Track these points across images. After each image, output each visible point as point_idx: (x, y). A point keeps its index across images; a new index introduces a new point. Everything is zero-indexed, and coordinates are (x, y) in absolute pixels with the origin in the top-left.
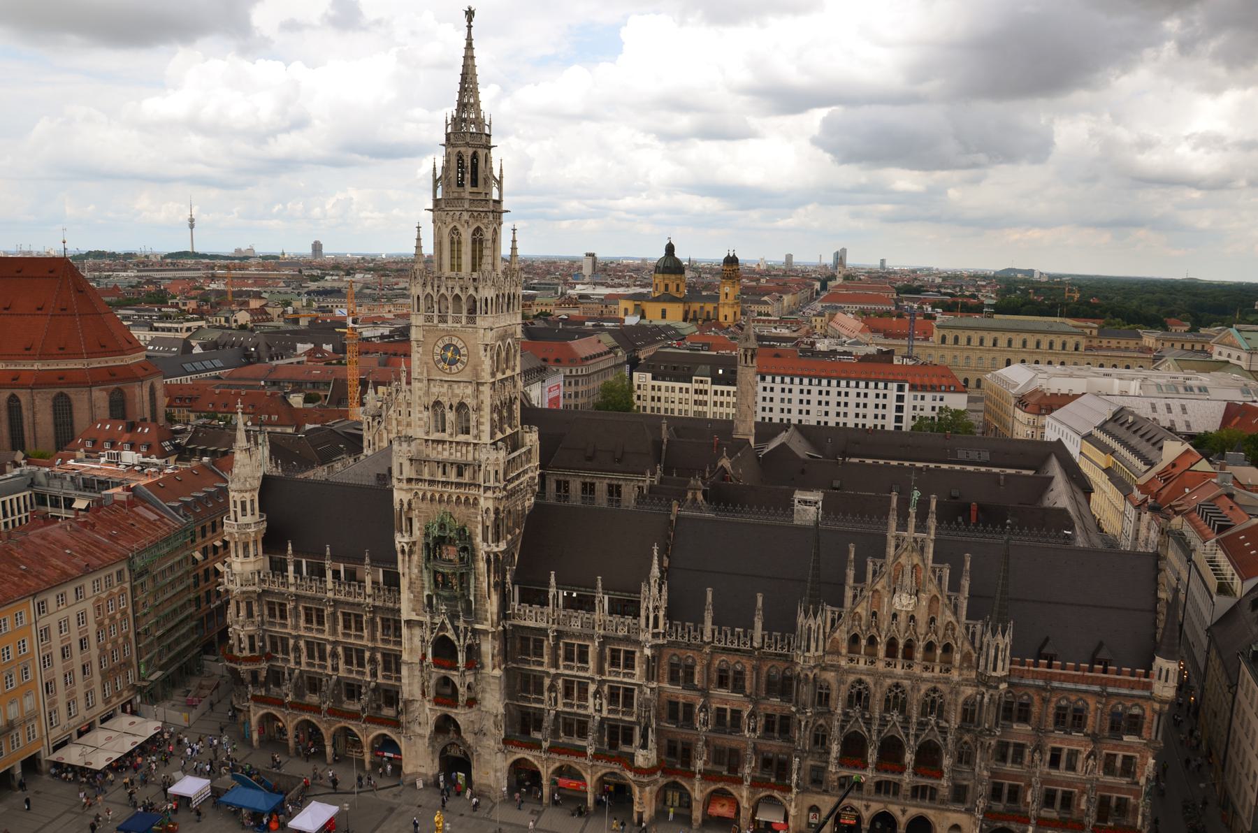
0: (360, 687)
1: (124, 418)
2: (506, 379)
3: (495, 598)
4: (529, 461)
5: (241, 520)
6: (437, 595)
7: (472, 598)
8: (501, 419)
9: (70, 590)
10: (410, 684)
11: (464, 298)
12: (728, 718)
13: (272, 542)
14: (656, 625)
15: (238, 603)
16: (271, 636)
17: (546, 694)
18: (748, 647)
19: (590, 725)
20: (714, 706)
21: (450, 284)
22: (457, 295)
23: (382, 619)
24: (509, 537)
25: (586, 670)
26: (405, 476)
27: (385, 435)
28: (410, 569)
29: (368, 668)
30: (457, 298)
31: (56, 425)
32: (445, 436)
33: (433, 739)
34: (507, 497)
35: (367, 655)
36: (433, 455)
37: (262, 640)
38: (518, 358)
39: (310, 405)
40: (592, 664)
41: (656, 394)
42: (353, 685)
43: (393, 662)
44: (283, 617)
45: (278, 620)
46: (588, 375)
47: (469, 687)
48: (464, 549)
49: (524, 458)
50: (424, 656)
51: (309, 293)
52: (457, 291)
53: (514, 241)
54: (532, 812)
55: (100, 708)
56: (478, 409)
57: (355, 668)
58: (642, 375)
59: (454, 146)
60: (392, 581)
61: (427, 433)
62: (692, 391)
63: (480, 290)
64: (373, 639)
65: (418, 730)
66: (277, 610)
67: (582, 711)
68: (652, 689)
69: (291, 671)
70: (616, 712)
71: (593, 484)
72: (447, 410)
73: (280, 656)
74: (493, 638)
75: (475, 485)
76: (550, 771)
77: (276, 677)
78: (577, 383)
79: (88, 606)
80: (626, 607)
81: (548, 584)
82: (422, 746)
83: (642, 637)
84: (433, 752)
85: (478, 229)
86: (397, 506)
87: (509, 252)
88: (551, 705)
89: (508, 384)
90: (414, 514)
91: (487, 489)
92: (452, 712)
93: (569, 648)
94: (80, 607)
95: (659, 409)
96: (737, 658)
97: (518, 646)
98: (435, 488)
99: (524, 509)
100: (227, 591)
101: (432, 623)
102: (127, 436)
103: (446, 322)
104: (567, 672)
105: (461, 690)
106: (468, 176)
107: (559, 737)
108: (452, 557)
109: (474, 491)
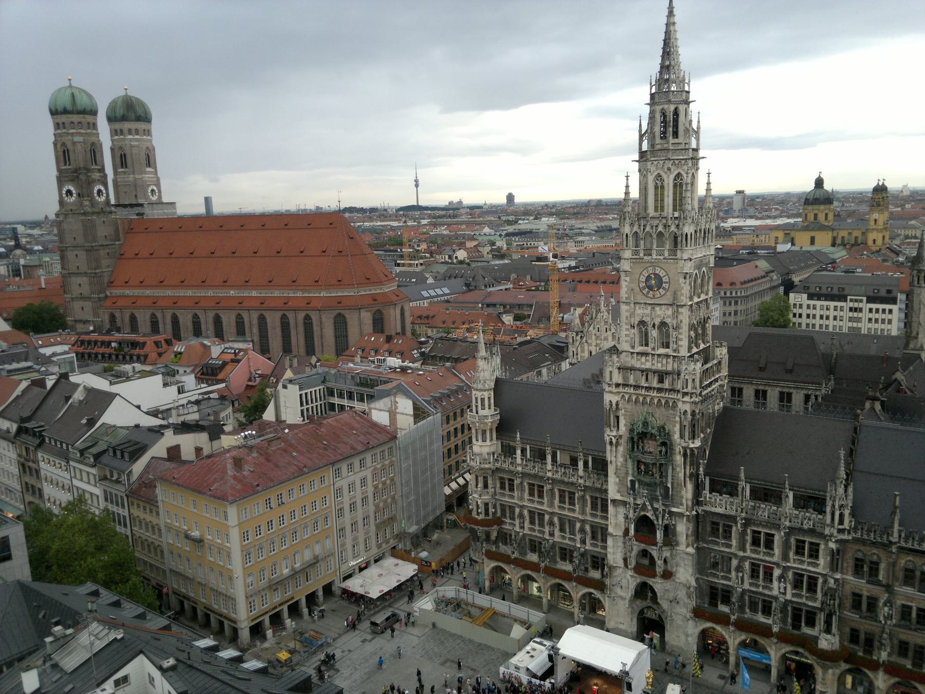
1: (383, 332)
3: (690, 486)
4: (719, 371)
6: (639, 481)
7: (669, 485)
8: (696, 336)
9: (356, 462)
10: (615, 553)
11: (667, 235)
13: (503, 429)
14: (841, 522)
16: (501, 505)
17: (733, 574)
19: (774, 604)
20: (899, 602)
21: (655, 222)
23: (591, 497)
24: (702, 435)
27: (586, 348)
28: (616, 458)
29: (578, 537)
30: (660, 235)
31: (336, 337)
33: (631, 602)
34: (702, 402)
35: (578, 525)
36: (638, 365)
37: (495, 507)
38: (711, 284)
39: (518, 323)
40: (777, 551)
41: (811, 312)
42: (565, 549)
43: (600, 533)
44: (511, 489)
45: (507, 492)
46: (747, 297)
47: (665, 561)
48: (663, 444)
50: (627, 532)
51: (508, 235)
52: (660, 228)
53: (709, 183)
55: (374, 551)
56: (677, 328)
58: (798, 295)
59: (659, 104)
60: (601, 466)
61: (633, 347)
62: (846, 309)
64: (583, 512)
65: (619, 591)
67: (767, 592)
68: (836, 580)
69: (518, 533)
70: (799, 596)
71: (765, 392)
72: (671, 330)
73: (508, 521)
74: (688, 520)
76: (737, 642)
77: (504, 537)
78: (736, 303)
79: (368, 473)
80: (812, 501)
85: (679, 175)
89: (703, 306)
90: (621, 413)
91: (685, 394)
92: (651, 581)
94: (362, 474)
95: (814, 325)
97: (709, 529)
98: (639, 392)
99: (714, 412)
101: (635, 504)
102: (386, 346)
103: (650, 255)
104: (754, 556)
105: (659, 563)
107: (744, 612)
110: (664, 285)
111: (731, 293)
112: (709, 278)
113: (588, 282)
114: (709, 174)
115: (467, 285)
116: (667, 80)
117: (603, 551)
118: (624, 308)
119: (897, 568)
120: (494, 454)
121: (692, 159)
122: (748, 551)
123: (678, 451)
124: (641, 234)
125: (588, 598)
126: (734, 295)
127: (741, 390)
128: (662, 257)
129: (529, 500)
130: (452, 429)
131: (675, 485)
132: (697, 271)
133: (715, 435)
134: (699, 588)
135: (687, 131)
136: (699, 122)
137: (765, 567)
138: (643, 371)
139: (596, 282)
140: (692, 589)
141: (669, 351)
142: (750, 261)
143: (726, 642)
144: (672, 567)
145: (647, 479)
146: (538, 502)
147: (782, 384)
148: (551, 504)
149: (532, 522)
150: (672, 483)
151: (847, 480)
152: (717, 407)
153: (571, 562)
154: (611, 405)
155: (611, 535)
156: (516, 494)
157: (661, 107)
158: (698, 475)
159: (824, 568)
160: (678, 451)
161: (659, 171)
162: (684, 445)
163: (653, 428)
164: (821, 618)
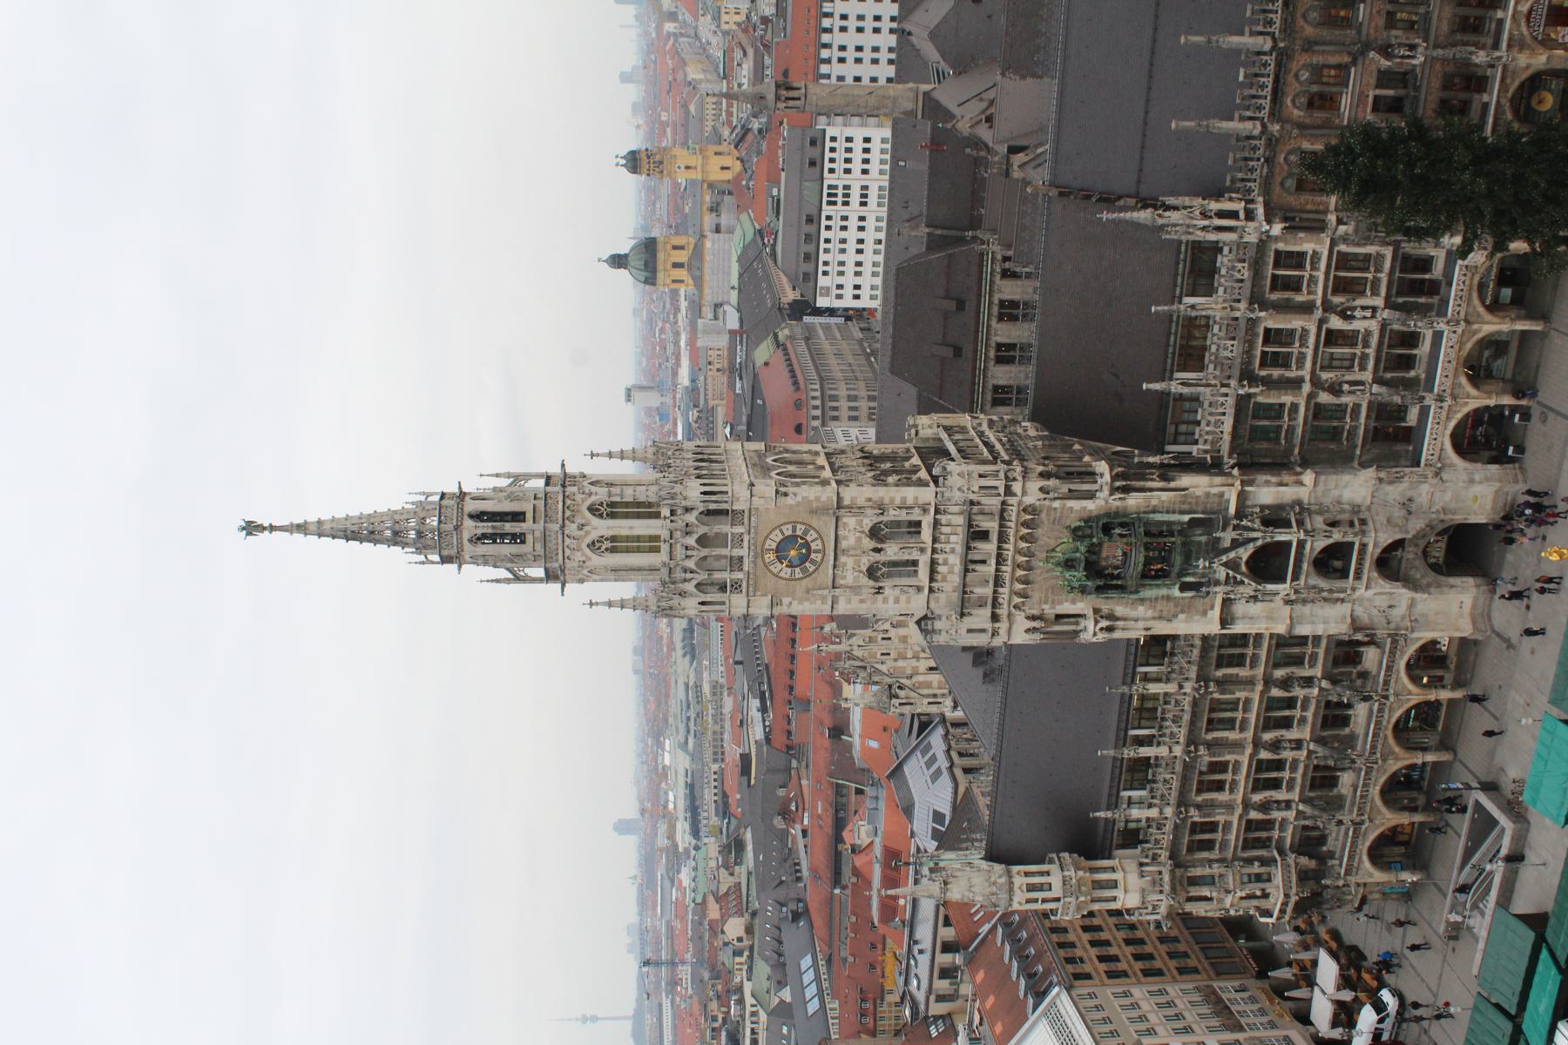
0: (1328, 704)
2: (831, 465)
3: (1186, 480)
4: (963, 430)
5: (1057, 891)
6: (1181, 574)
7: (1186, 518)
8: (897, 472)
10: (1326, 620)
11: (702, 530)
12: (1391, 92)
13: (1090, 842)
14: (1233, 215)
15: (1190, 899)
16: (1244, 848)
17: (1345, 399)
18: (1271, 60)
19: (1396, 327)
20: (1370, 117)
21: (679, 552)
22: (698, 541)
23: (1219, 666)
24: (1087, 459)
25: (1305, 332)
26: (988, 625)
27: (921, 678)
28: (1139, 617)
29: (1299, 692)
30: (703, 541)
32: (924, 560)
34: (1022, 460)
35: (1276, 692)
36: (955, 579)
40: (1296, 323)
42: (1325, 718)
43: (1289, 648)
44: (1212, 827)
45: (1218, 836)
46: (822, 379)
49: (958, 437)
51: (695, 832)
52: (691, 541)
53: (610, 455)
54: (1544, 420)
56: (882, 508)
57: (1297, 713)
60: (1157, 647)
61: (919, 589)
63: (688, 504)
64: (1250, 682)
65: (1401, 610)
66: (1201, 836)
67: (1374, 341)
68: (1340, 222)
69: (1300, 814)
71: (999, 346)
72: (885, 518)
73: (1276, 834)
74: (1251, 483)
75: (1003, 511)
76: (1473, 392)
80: (1200, 266)
81: (1165, 394)
82: (1427, 603)
83: (1252, 238)
84: (1439, 586)
85: (592, 509)
86: (1036, 638)
87: (628, 463)
88: (1361, 392)
90: (1050, 611)
91: (1008, 491)
92: (1372, 552)
93: (1269, 360)
95: (875, 264)
96: (1290, 78)
97: (1265, 445)
98: (1007, 576)
100: (1169, 916)
101: (1227, 582)
103: (741, 559)
104: (1308, 364)
105: (1337, 536)
106: (509, 527)
107: (1417, 380)
108: (1120, 552)
109: (1013, 513)
110: (799, 533)
111: (816, 407)
112: (787, 451)
113: (792, 673)
114: (592, 455)
115: (796, 917)
116: (420, 534)
117: (1324, 643)
118: (843, 608)
119: (1308, 121)
120: (1141, 865)
121: (564, 486)
122: (1300, 373)
123: (1118, 503)
124: (702, 576)
125: (1418, 672)
126: (818, 402)
127: (996, 388)
128: (746, 538)
129: (1231, 791)
130: (1093, 952)
131: (1186, 507)
132: (773, 474)
133: (1083, 435)
134: (1380, 462)
135: (512, 497)
136: (497, 475)
137: (1328, 343)
138: (966, 570)
139: (793, 657)
140: (1382, 475)
141: (927, 521)
142: (755, 376)
143: (1476, 411)
144: (1343, 511)
145: (1178, 560)
146: (1234, 773)
147: (984, 317)
148: (1237, 746)
149: (1275, 784)
150: (1182, 512)
151: (1155, 207)
152: (1032, 433)
153: (1349, 706)
154: (1034, 630)
155: (1292, 626)
156: (1221, 818)
157: (466, 542)
158: (1162, 465)
159: (1321, 242)
160: (1118, 503)
161: (584, 546)
162: (1106, 491)
163: (1077, 550)
164: (1410, 248)
